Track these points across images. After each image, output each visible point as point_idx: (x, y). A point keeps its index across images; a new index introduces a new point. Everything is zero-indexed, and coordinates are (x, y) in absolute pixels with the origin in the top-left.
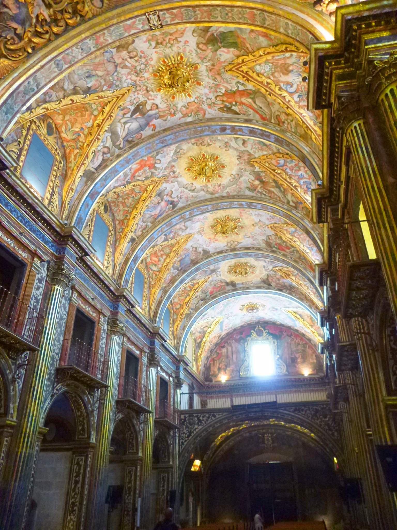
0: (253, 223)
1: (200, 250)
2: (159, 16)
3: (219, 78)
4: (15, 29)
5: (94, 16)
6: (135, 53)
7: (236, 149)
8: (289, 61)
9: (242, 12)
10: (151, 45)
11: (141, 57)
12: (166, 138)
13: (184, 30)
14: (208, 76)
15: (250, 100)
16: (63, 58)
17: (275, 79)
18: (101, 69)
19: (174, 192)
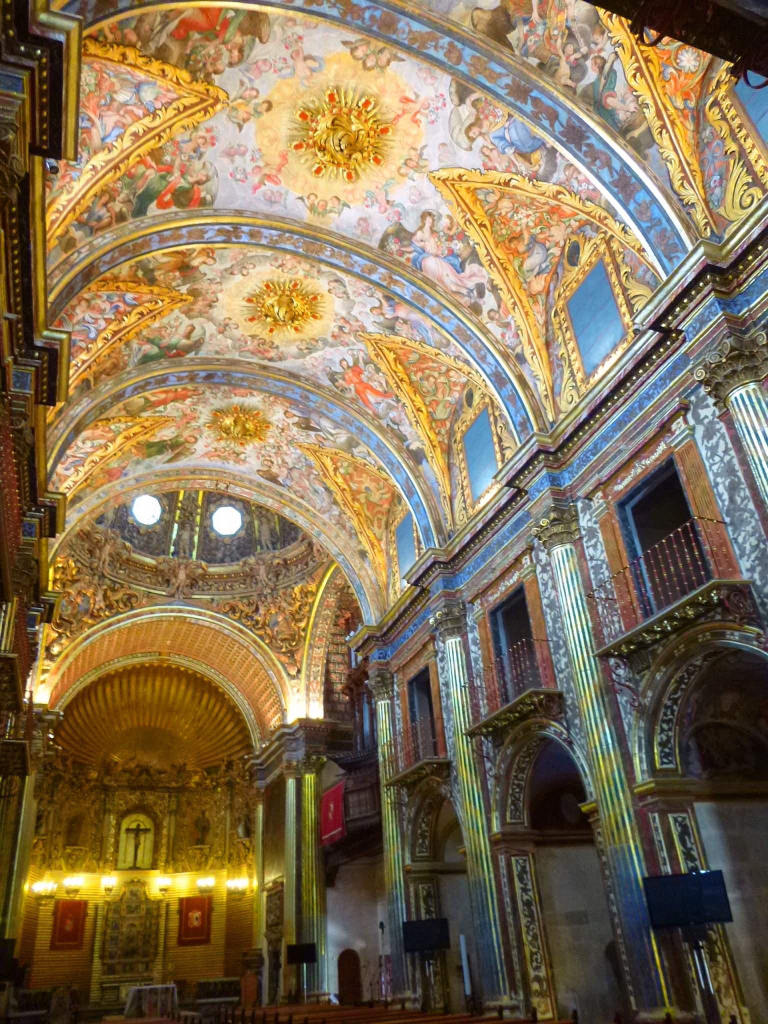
0: (265, 117)
1: (467, 111)
3: (188, 411)
15: (153, 399)
19: (369, 307)
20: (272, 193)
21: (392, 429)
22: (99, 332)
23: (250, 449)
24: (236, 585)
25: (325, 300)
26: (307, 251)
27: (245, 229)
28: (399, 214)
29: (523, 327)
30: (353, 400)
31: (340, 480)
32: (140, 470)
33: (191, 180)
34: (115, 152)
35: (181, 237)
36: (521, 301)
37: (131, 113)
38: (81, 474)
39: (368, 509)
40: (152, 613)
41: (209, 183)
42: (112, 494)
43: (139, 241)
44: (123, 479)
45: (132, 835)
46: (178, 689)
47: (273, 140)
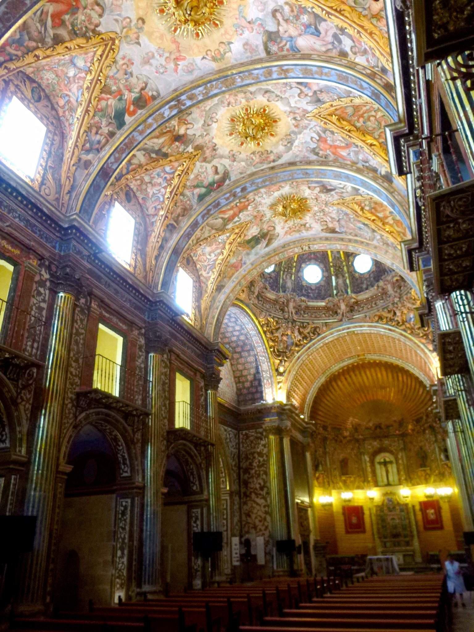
0: (146, 27)
3: (255, 214)
7: (221, 157)
12: (302, 176)
15: (226, 216)
19: (296, 95)
20: (187, 66)
21: (367, 167)
22: (163, 196)
23: (308, 218)
24: (378, 302)
25: (271, 108)
26: (227, 87)
27: (183, 97)
28: (261, 25)
29: (372, 45)
30: (335, 161)
31: (369, 215)
32: (252, 257)
33: (137, 90)
34: (83, 103)
35: (150, 125)
36: (362, 27)
37: (80, 78)
38: (215, 273)
39: (398, 226)
40: (332, 334)
41: (149, 86)
42: (240, 278)
43: (126, 141)
44: (244, 267)
45: (383, 466)
46: (382, 375)
47: (162, 37)
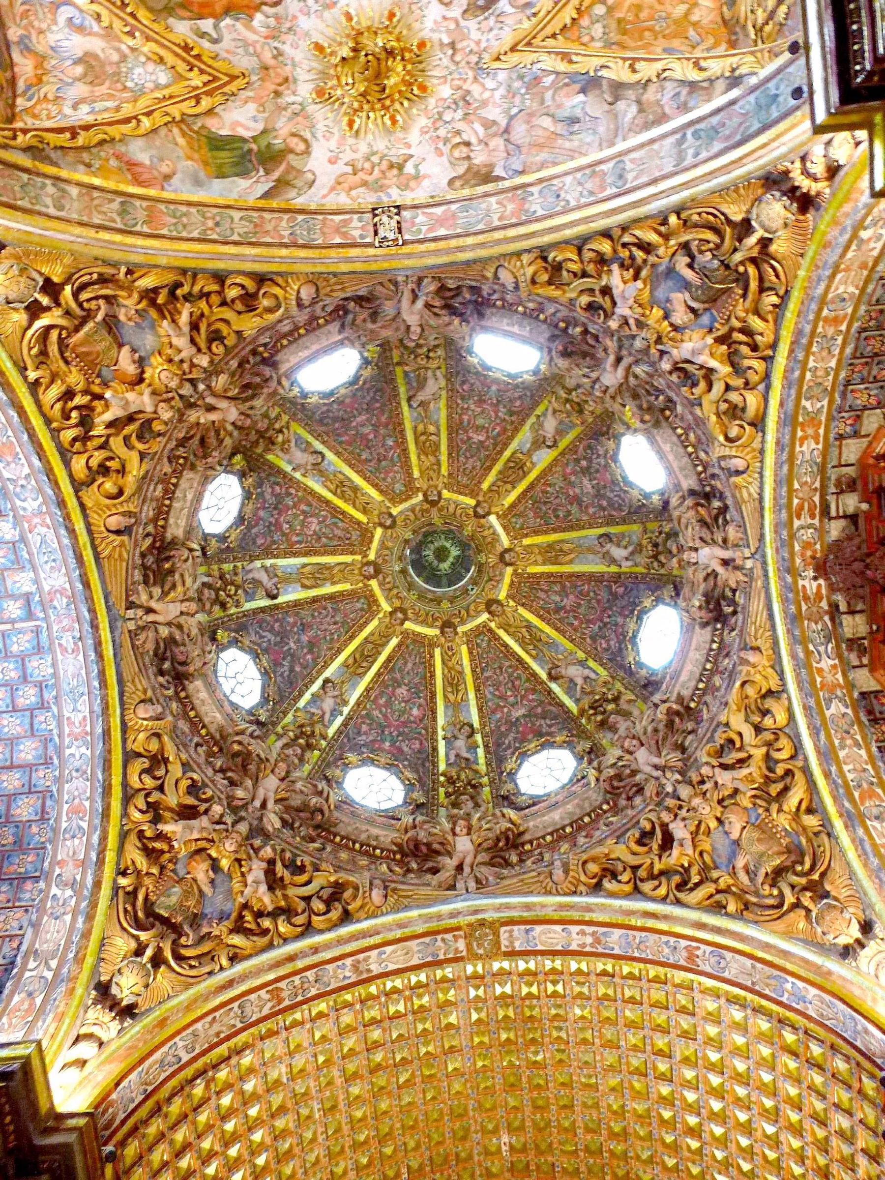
2: (376, 233)
3: (267, 57)
4: (690, 266)
5: (518, 254)
6: (457, 154)
8: (80, 90)
9: (180, 227)
10: (416, 166)
11: (446, 141)
13: (333, 189)
14: (294, 65)
16: (603, 189)
17: (117, 44)
18: (540, 132)
